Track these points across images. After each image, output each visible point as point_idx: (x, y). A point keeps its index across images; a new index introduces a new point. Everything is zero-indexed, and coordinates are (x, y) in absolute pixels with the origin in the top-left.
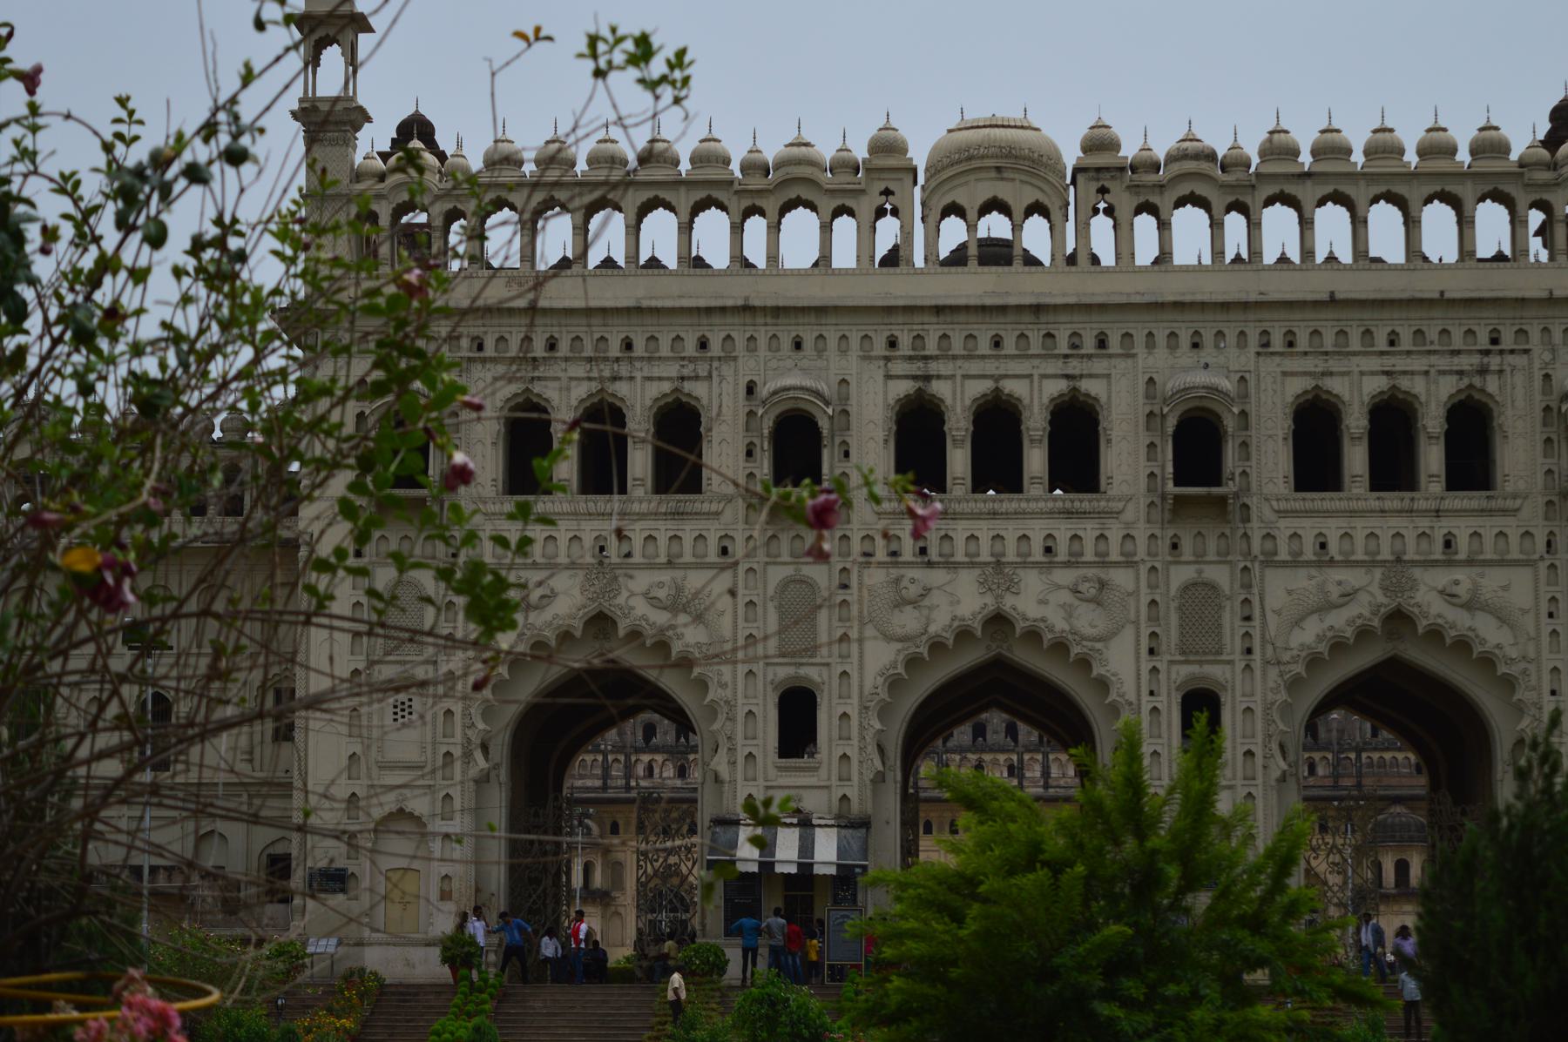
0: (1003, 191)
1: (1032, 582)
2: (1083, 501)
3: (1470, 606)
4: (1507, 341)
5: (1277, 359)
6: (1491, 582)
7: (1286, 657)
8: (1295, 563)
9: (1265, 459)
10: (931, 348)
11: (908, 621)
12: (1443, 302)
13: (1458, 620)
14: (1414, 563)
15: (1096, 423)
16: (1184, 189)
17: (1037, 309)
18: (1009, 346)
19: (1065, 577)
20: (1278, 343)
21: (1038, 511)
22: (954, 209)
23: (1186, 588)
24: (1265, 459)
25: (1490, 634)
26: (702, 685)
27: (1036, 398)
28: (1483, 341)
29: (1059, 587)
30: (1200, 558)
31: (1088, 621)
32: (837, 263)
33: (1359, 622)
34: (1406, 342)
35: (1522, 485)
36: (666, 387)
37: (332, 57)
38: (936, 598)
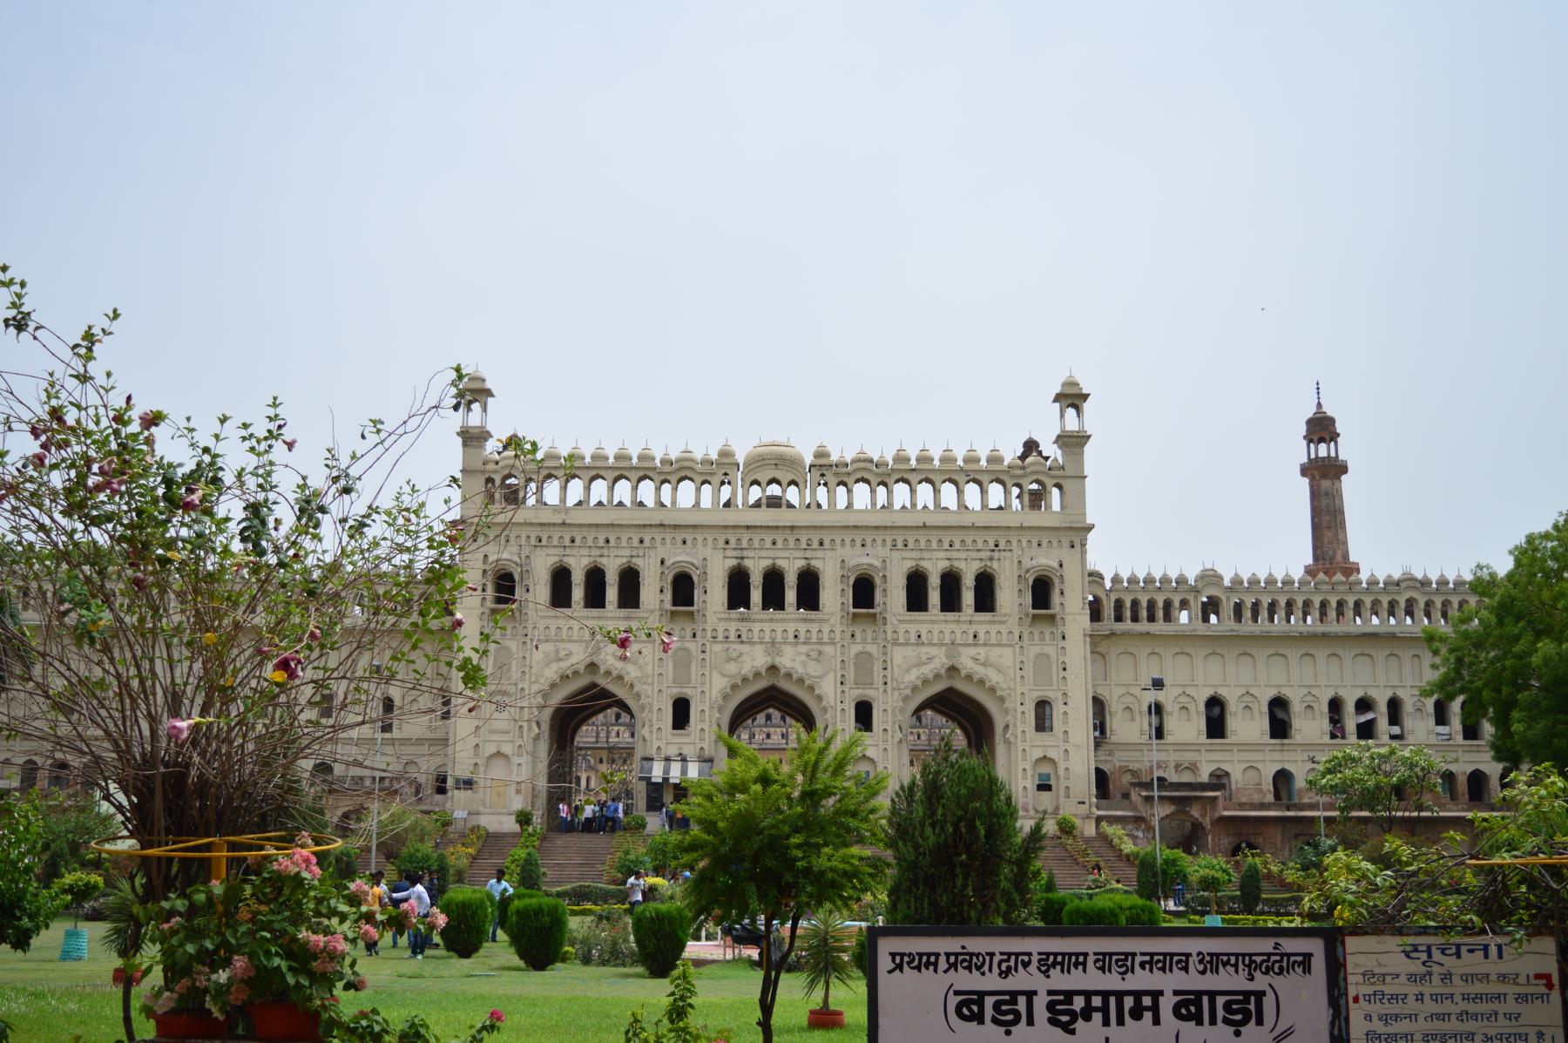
0: (778, 475)
1: (788, 651)
2: (812, 614)
3: (984, 664)
4: (1002, 545)
6: (995, 653)
8: (906, 644)
9: (893, 596)
10: (745, 545)
11: (732, 668)
12: (974, 527)
13: (980, 671)
15: (818, 580)
16: (859, 475)
17: (792, 528)
18: (779, 545)
19: (803, 649)
20: (900, 545)
21: (792, 616)
22: (756, 482)
24: (893, 596)
25: (994, 677)
26: (638, 696)
28: (992, 546)
30: (864, 641)
31: (813, 669)
32: (856, 506)
34: (957, 545)
36: (624, 560)
37: (476, 407)
38: (745, 658)
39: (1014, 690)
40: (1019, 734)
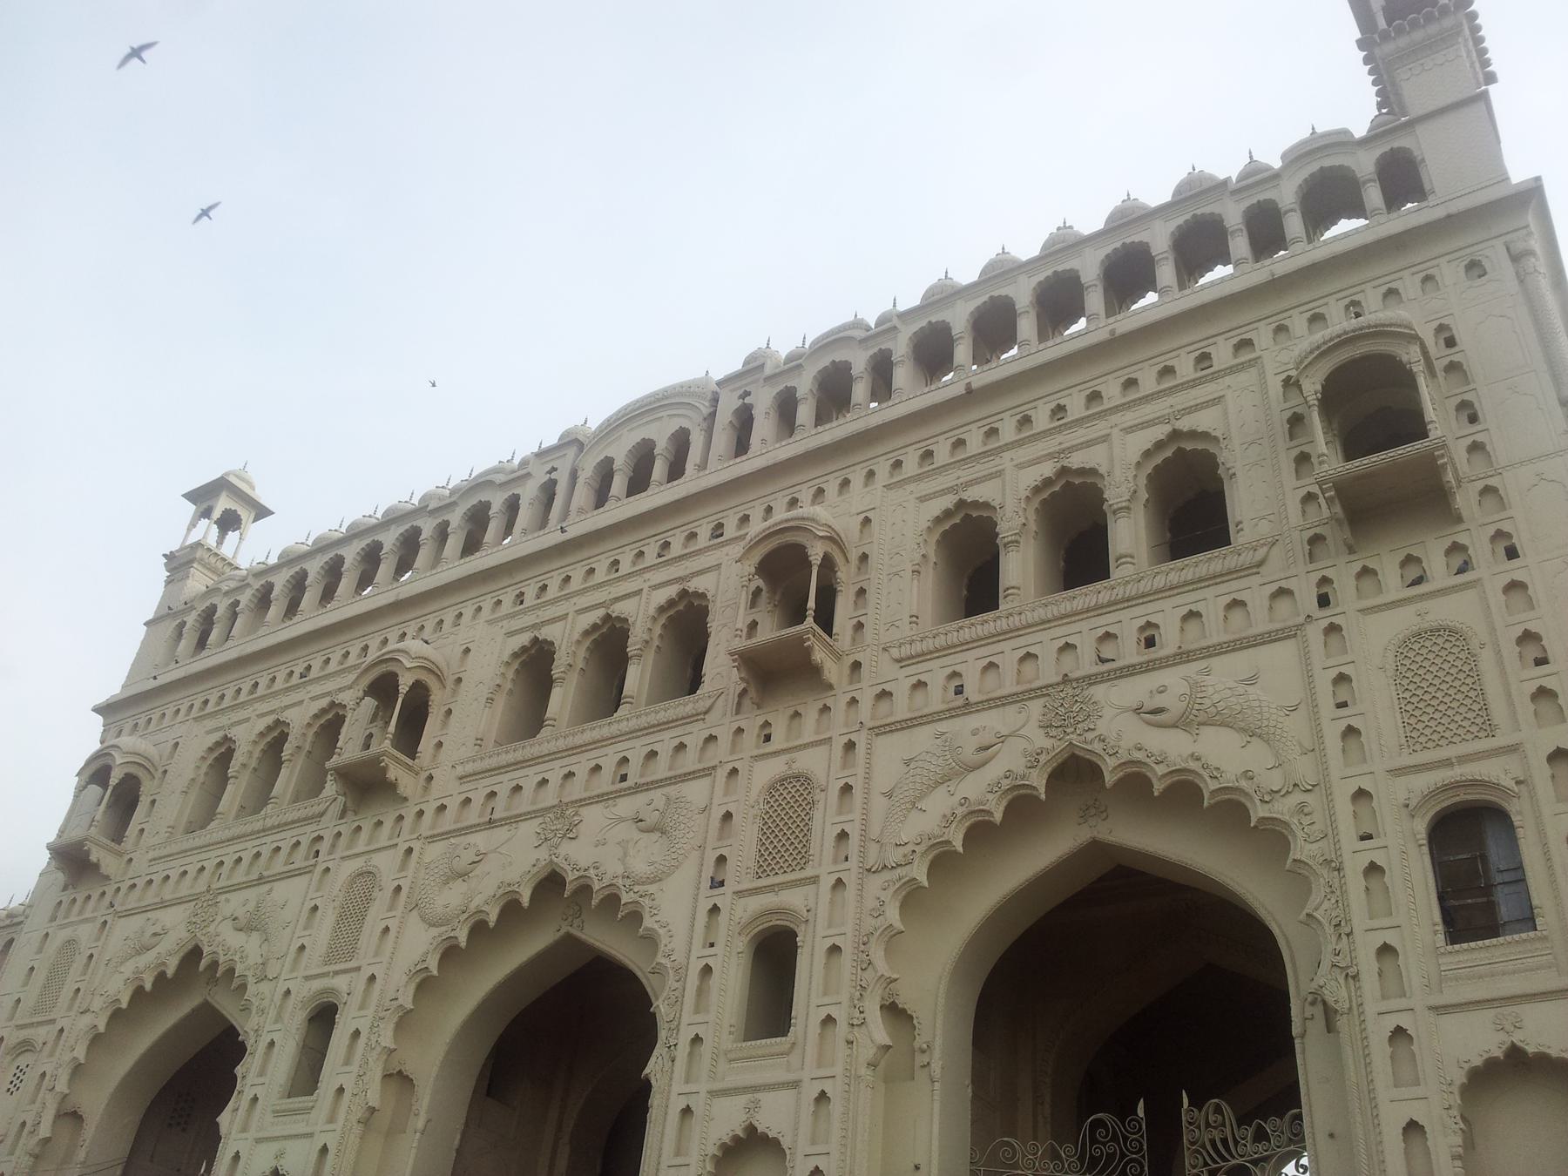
1: (593, 816)
3: (1184, 723)
5: (912, 487)
7: (894, 856)
11: (451, 898)
13: (1170, 749)
14: (1092, 680)
19: (626, 806)
23: (772, 788)
25: (1224, 758)
27: (642, 615)
29: (622, 820)
33: (1006, 784)
35: (1265, 528)
39: (1321, 786)
40: (1367, 962)
